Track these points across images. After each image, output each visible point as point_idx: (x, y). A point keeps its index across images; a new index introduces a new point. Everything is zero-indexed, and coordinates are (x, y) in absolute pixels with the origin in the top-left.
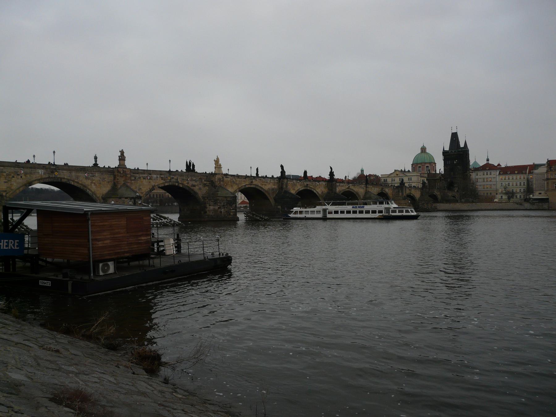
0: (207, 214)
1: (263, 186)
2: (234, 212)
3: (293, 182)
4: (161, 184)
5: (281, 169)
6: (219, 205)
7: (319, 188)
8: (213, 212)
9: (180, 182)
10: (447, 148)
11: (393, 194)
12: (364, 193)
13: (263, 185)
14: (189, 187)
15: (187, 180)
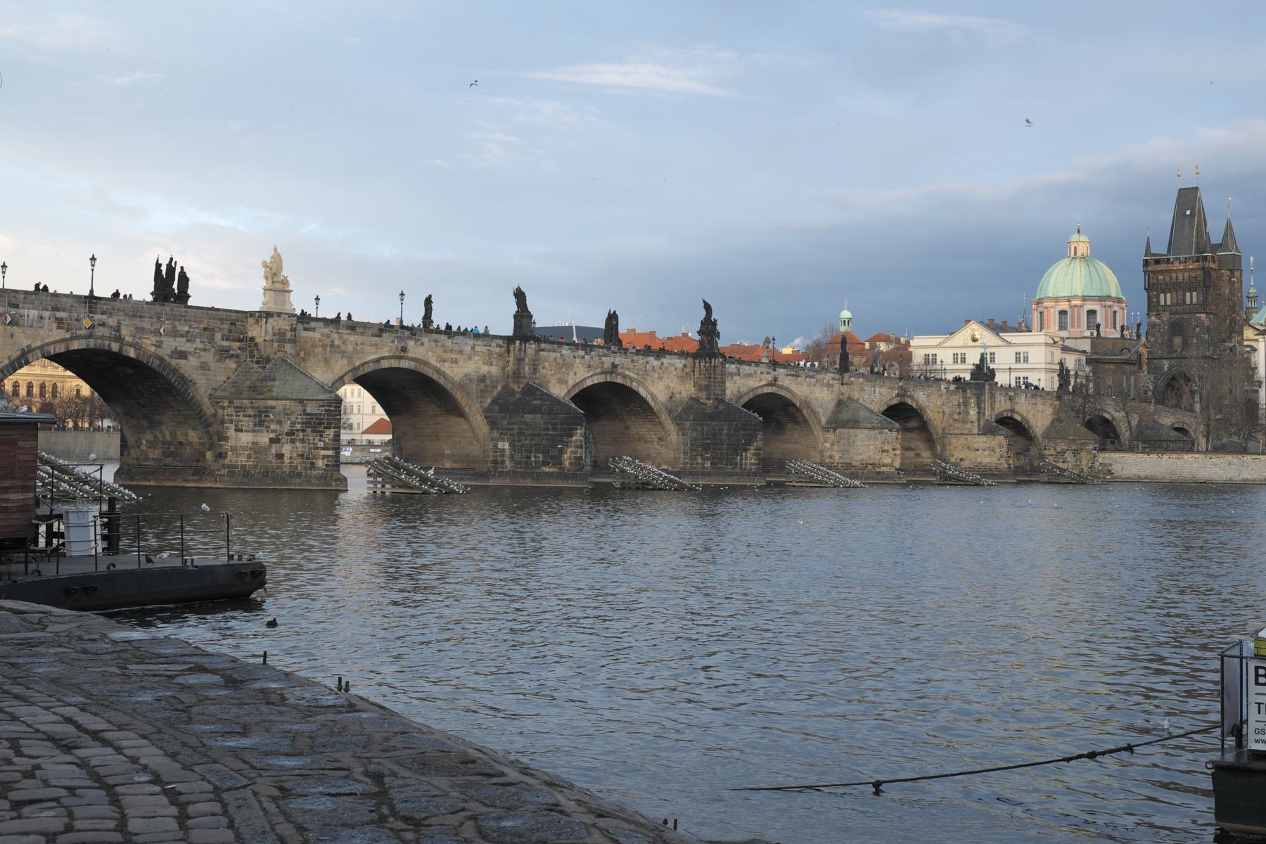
0: (227, 461)
1: (446, 364)
2: (328, 457)
3: (558, 355)
4: (55, 342)
5: (517, 304)
6: (273, 431)
7: (661, 378)
8: (249, 457)
9: (128, 339)
10: (1160, 248)
11: (943, 412)
12: (834, 404)
13: (444, 361)
14: (161, 359)
15: (157, 332)
